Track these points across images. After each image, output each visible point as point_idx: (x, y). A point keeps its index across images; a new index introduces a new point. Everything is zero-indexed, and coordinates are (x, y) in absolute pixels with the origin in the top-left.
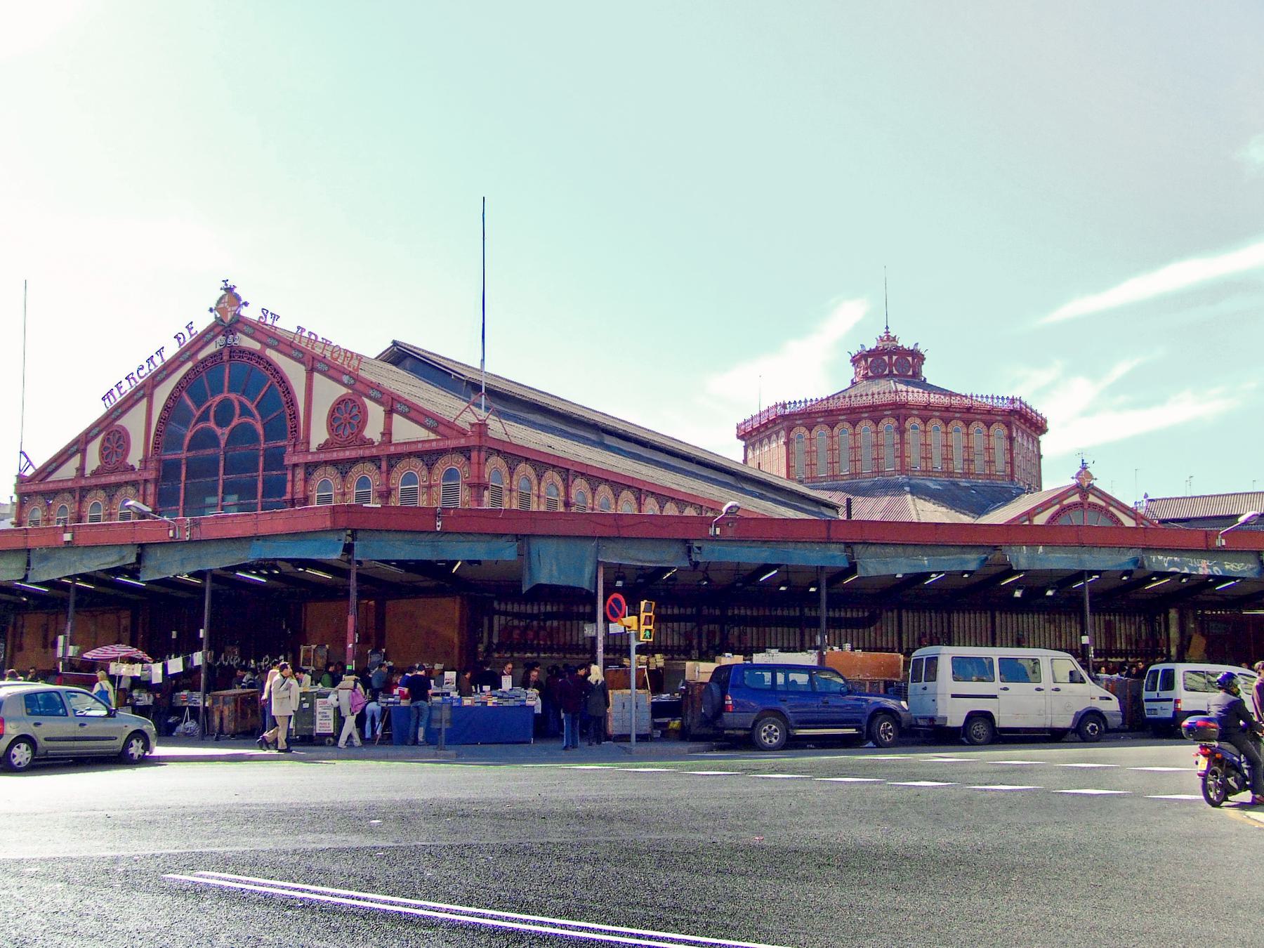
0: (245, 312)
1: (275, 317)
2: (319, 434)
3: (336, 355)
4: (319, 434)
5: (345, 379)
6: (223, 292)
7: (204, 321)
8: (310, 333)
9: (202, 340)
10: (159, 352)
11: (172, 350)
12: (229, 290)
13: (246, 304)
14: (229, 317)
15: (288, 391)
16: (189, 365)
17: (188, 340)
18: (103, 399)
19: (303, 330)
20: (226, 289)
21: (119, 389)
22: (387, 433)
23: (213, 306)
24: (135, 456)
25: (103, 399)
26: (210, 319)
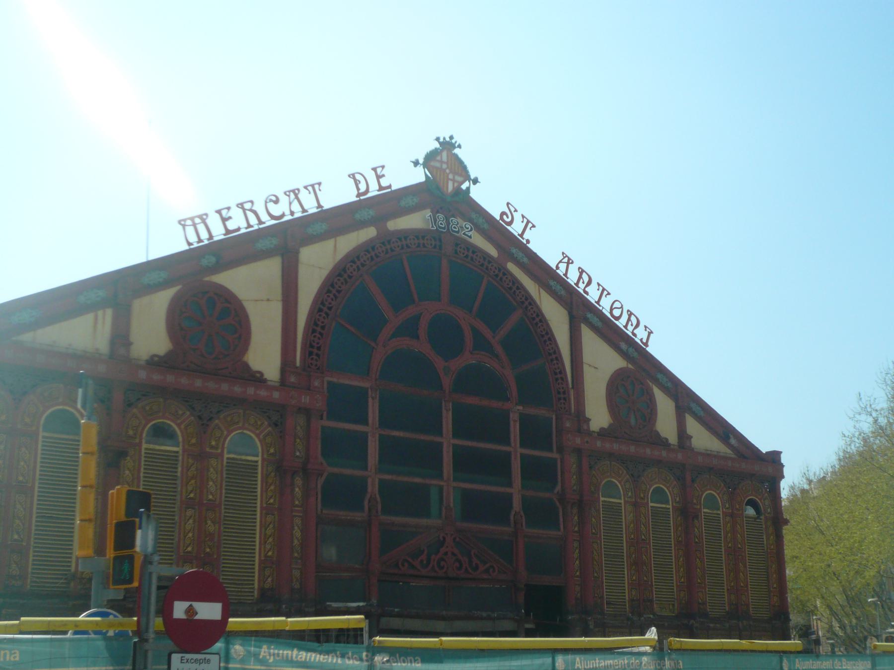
0: (477, 194)
1: (528, 224)
2: (598, 416)
3: (617, 313)
4: (598, 416)
5: (623, 346)
6: (437, 145)
7: (406, 175)
8: (581, 271)
9: (392, 202)
10: (314, 188)
11: (338, 194)
12: (448, 145)
13: (475, 181)
14: (450, 188)
15: (548, 336)
16: (370, 233)
17: (374, 192)
18: (182, 223)
19: (570, 262)
20: (440, 143)
21: (224, 220)
22: (683, 435)
23: (421, 161)
24: (265, 355)
25: (182, 223)
26: (418, 176)
